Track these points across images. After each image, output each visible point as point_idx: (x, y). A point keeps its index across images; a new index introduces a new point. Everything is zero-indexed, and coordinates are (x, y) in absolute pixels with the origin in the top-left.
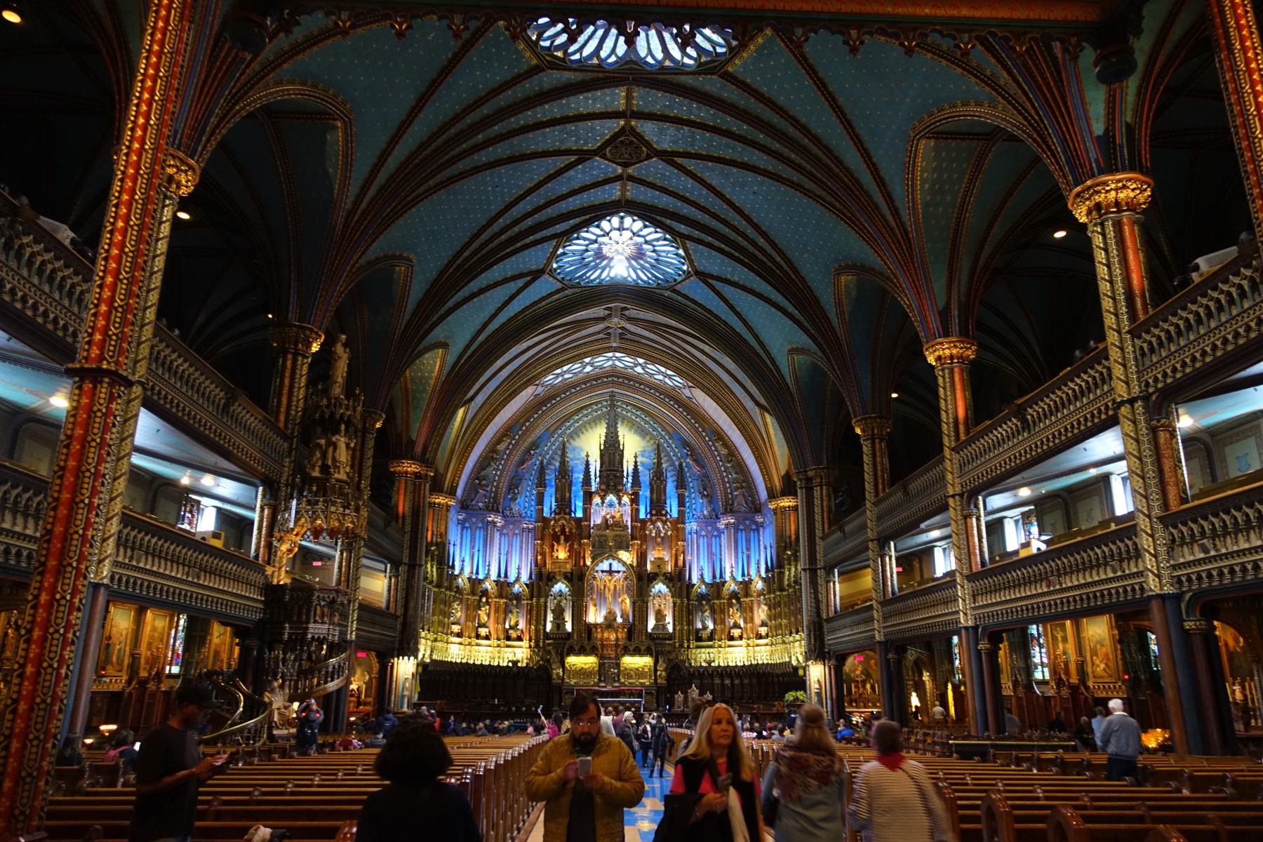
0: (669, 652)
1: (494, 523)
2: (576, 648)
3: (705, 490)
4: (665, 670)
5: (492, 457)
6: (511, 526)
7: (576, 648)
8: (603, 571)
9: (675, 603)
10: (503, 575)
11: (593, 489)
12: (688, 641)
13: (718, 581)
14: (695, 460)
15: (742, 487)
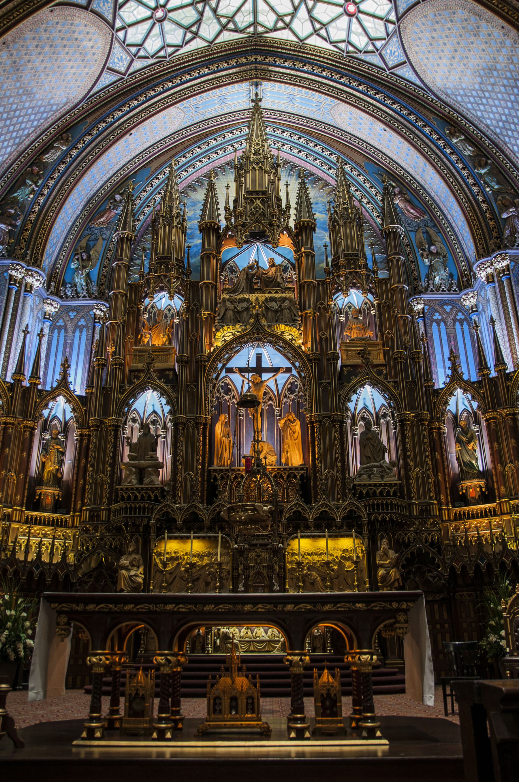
0: (401, 525)
1: (29, 289)
2: (179, 519)
3: (431, 243)
4: (395, 565)
5: (32, 173)
6: (72, 315)
7: (179, 519)
8: (242, 370)
9: (402, 422)
10: (28, 371)
11: (223, 223)
12: (440, 510)
13: (493, 374)
14: (408, 201)
15: (514, 205)
